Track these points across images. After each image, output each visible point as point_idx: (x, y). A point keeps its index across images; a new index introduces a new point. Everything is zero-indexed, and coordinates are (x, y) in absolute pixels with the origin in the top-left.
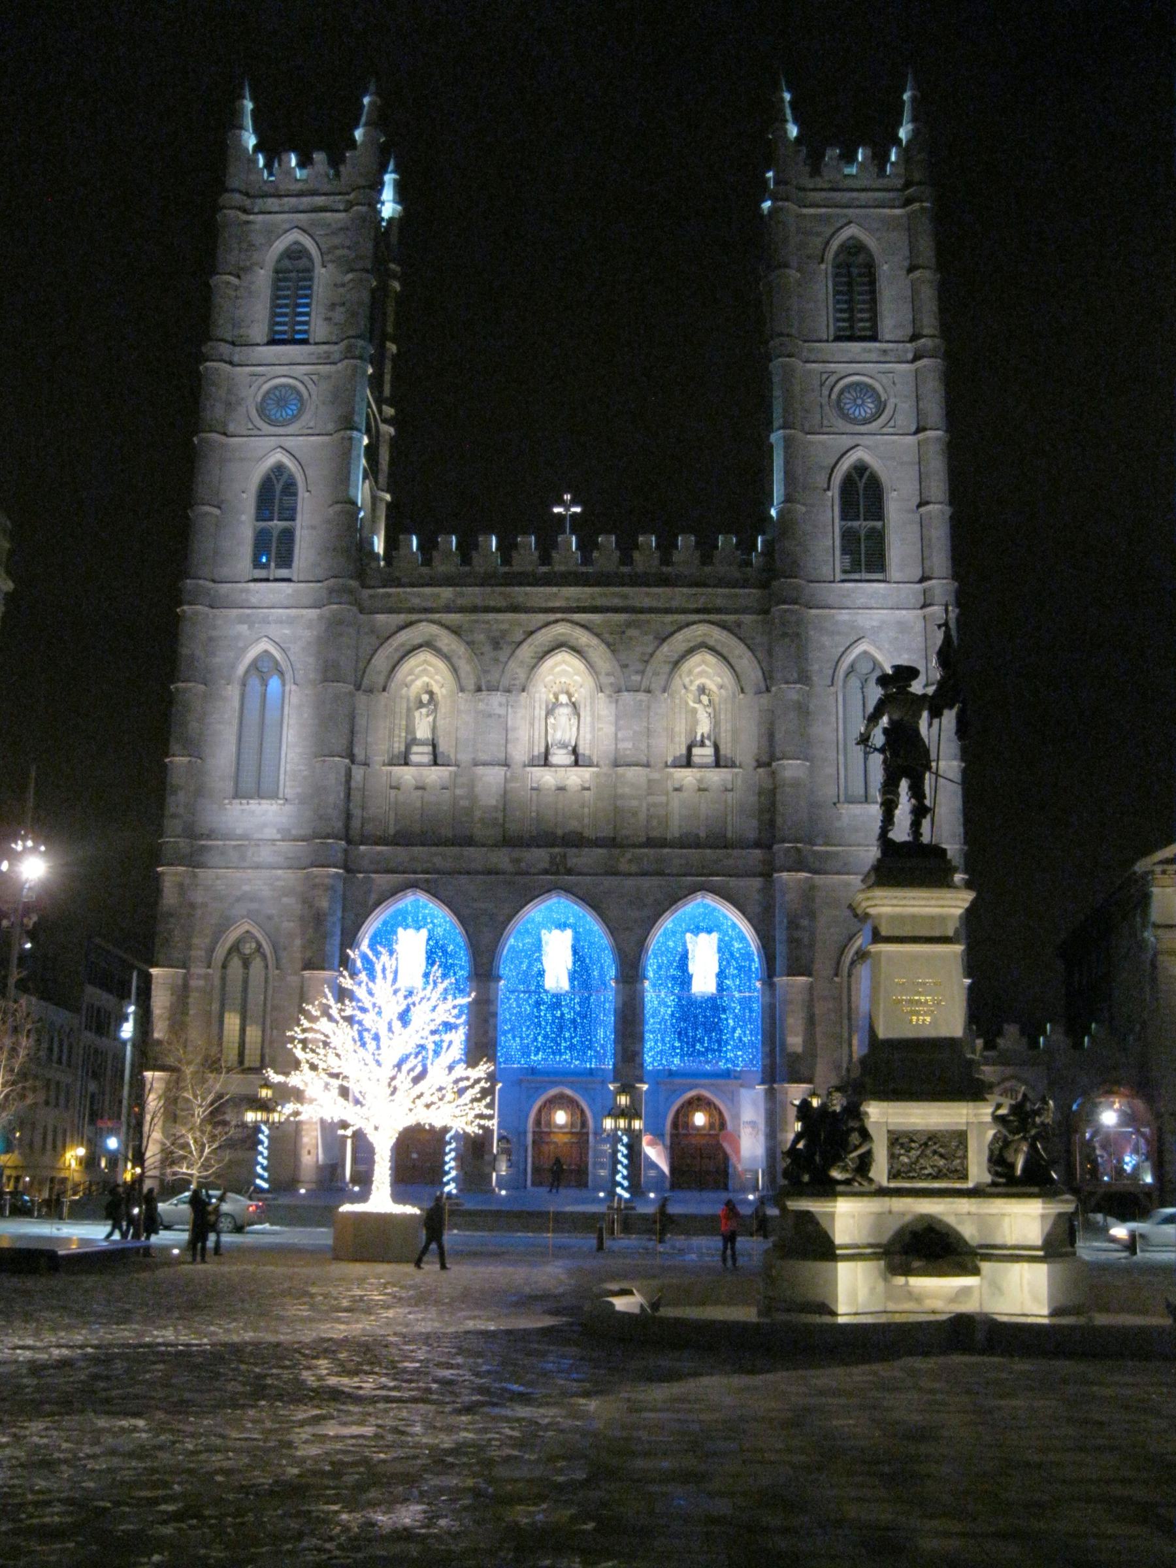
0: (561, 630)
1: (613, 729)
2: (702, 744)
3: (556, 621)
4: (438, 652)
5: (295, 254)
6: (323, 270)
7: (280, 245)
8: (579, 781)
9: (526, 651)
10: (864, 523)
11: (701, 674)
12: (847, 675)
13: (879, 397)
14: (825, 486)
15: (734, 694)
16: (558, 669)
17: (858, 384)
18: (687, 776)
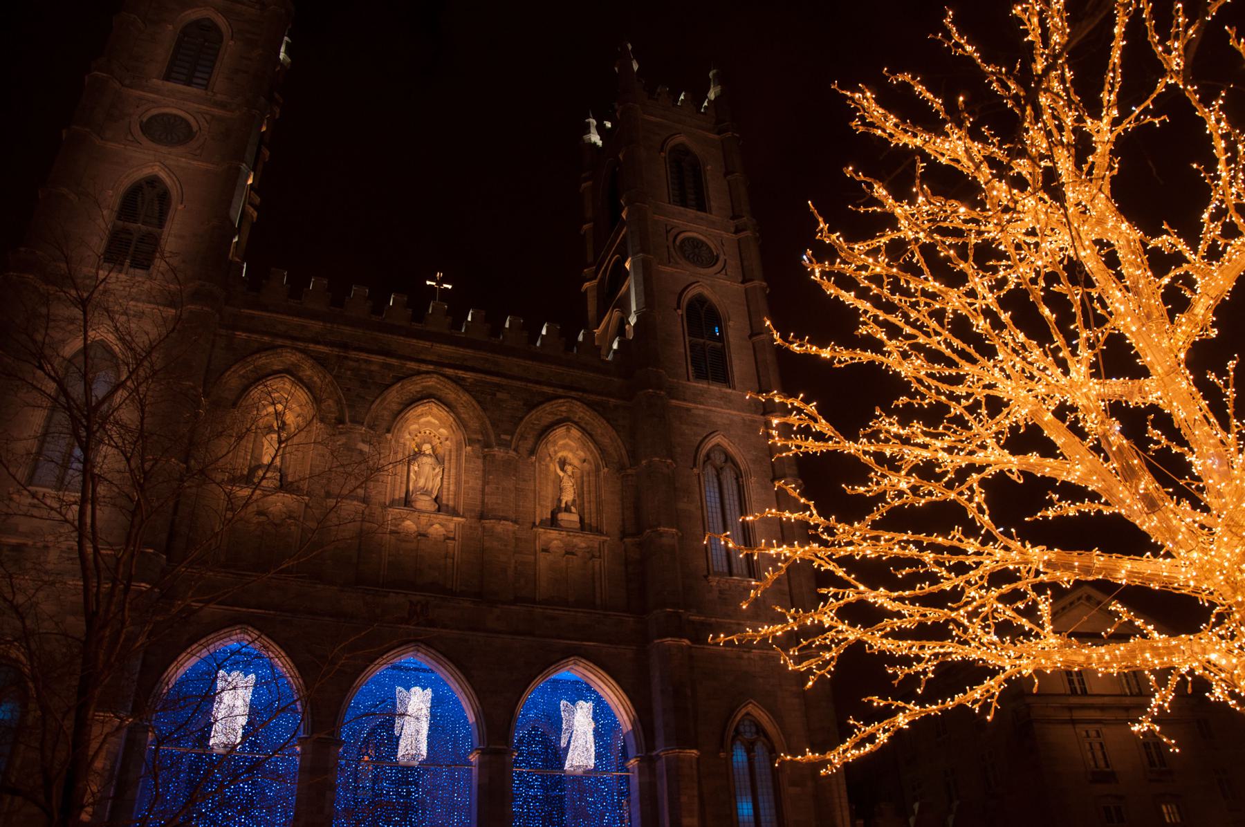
0: (431, 382)
1: (480, 483)
2: (567, 510)
3: (427, 373)
4: (300, 381)
5: (206, 28)
6: (231, 43)
7: (193, 14)
8: (442, 530)
9: (394, 396)
10: (708, 342)
11: (564, 447)
12: (704, 462)
13: (711, 252)
14: (675, 306)
15: (598, 470)
16: (423, 420)
17: (694, 239)
18: (554, 538)
